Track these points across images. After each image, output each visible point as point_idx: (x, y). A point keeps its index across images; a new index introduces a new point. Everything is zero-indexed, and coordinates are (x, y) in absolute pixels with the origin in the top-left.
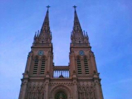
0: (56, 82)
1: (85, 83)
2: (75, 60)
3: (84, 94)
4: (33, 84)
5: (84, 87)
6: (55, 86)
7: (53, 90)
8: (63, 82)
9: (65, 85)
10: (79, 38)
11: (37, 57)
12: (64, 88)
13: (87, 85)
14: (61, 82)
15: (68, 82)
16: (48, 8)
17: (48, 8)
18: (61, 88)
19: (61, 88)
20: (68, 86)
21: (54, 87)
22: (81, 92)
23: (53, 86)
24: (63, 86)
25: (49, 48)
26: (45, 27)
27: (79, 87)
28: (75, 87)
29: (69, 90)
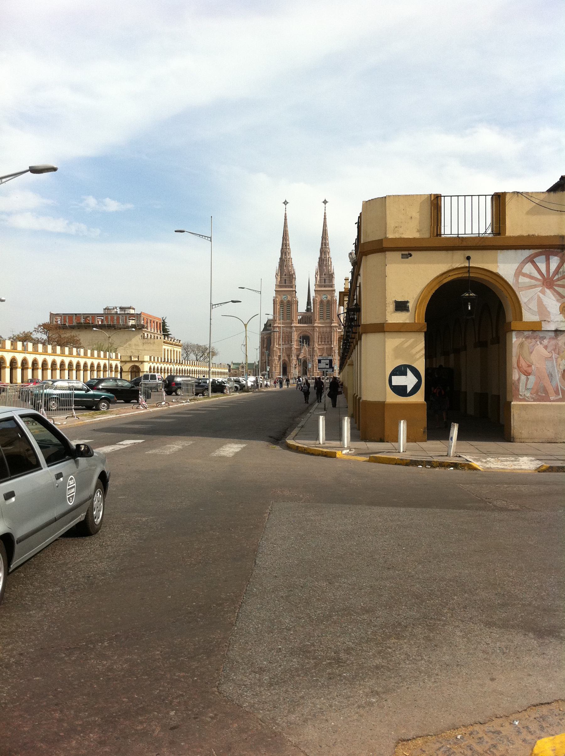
1: (325, 329)
3: (323, 338)
8: (307, 328)
9: (308, 331)
12: (307, 333)
13: (326, 330)
15: (311, 328)
16: (286, 205)
17: (286, 205)
18: (305, 333)
20: (311, 332)
21: (299, 333)
23: (299, 331)
24: (306, 332)
25: (293, 291)
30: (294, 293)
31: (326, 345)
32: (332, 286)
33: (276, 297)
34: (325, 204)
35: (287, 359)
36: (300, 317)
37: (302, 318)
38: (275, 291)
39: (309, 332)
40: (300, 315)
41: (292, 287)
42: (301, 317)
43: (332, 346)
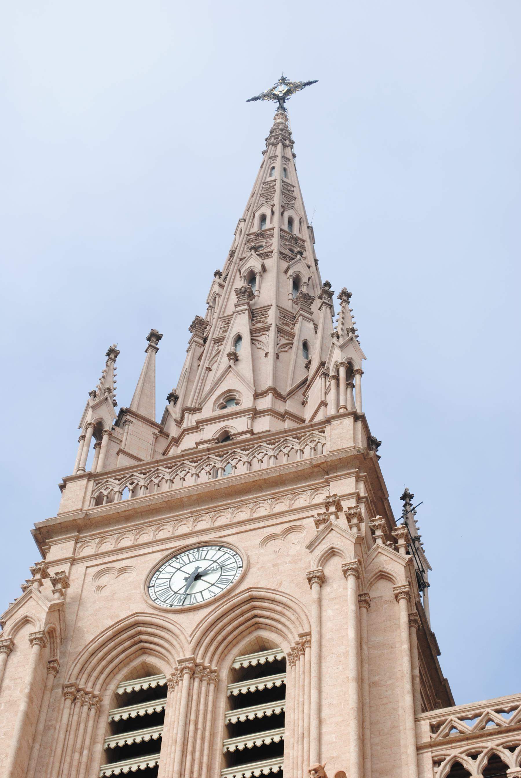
16: (281, 99)
26: (251, 278)
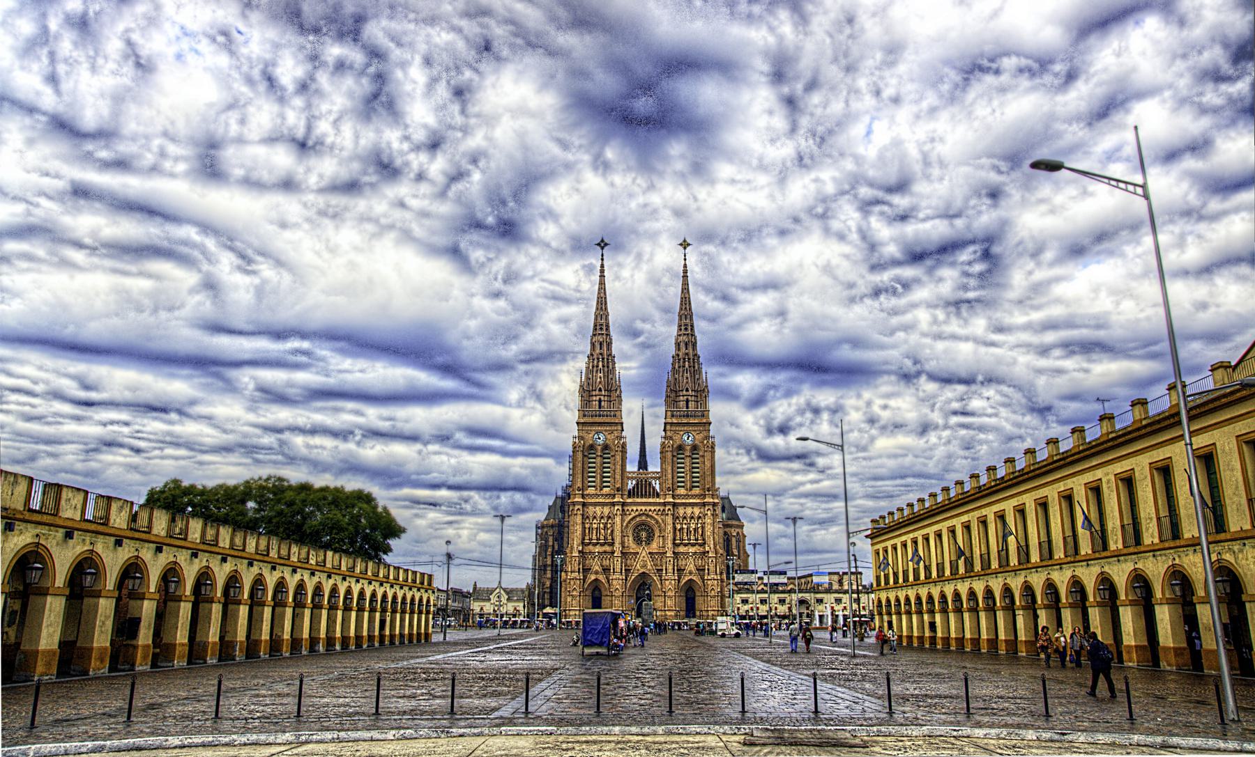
0: (635, 508)
1: (689, 510)
2: (673, 456)
4: (591, 510)
5: (685, 518)
6: (633, 514)
7: (629, 522)
8: (648, 508)
10: (687, 390)
11: (592, 447)
14: (643, 508)
15: (657, 508)
18: (644, 518)
19: (644, 518)
22: (679, 527)
24: (648, 516)
25: (616, 424)
27: (675, 518)
28: (669, 520)
29: (657, 522)
30: (620, 428)
31: (693, 545)
32: (705, 413)
33: (581, 438)
34: (685, 248)
35: (602, 578)
36: (631, 484)
37: (637, 484)
38: (578, 423)
39: (652, 517)
40: (632, 478)
41: (615, 416)
42: (634, 482)
43: (707, 549)
